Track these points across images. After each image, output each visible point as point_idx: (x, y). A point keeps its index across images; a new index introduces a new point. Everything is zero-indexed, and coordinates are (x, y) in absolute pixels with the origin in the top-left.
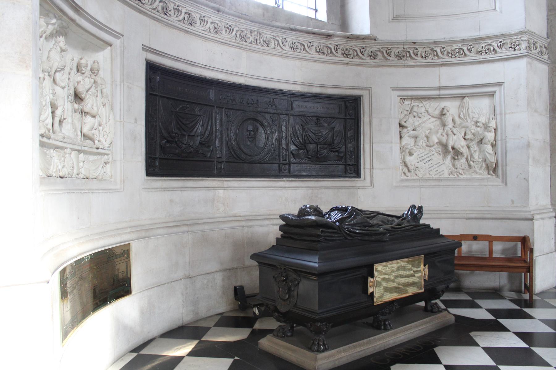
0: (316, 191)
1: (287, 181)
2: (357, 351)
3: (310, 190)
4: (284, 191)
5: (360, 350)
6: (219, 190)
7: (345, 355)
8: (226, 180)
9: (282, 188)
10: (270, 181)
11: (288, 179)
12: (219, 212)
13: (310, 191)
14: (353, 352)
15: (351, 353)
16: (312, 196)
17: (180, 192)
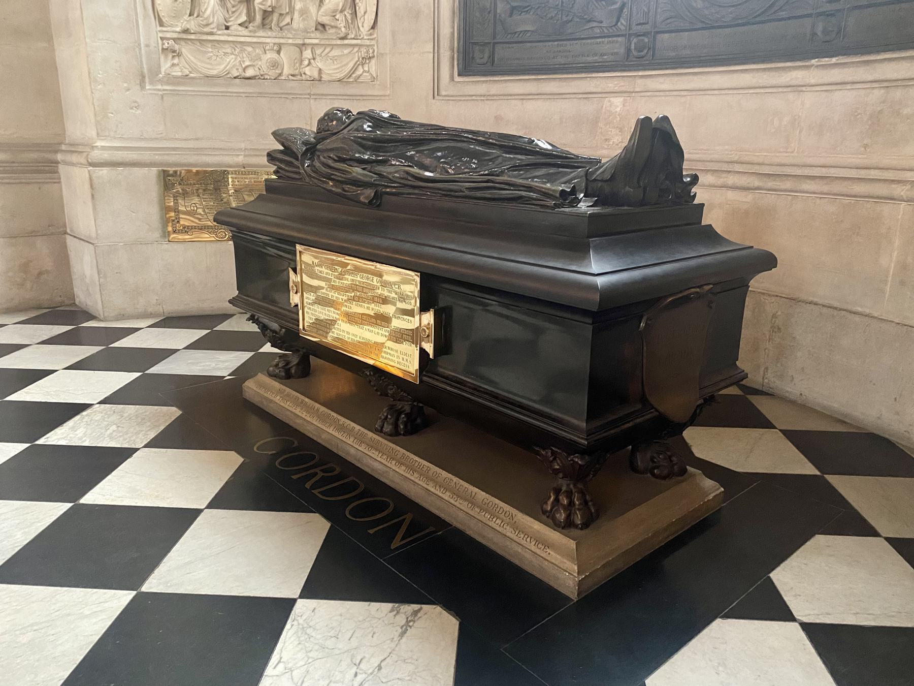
0: (898, 94)
1: (817, 66)
2: (294, 411)
3: (876, 91)
4: (791, 96)
5: (300, 414)
6: (611, 99)
7: (278, 402)
8: (642, 77)
9: (789, 89)
10: (764, 70)
11: (826, 61)
12: (608, 145)
13: (878, 94)
14: (289, 408)
15: (286, 406)
16: (881, 112)
17: (518, 103)
